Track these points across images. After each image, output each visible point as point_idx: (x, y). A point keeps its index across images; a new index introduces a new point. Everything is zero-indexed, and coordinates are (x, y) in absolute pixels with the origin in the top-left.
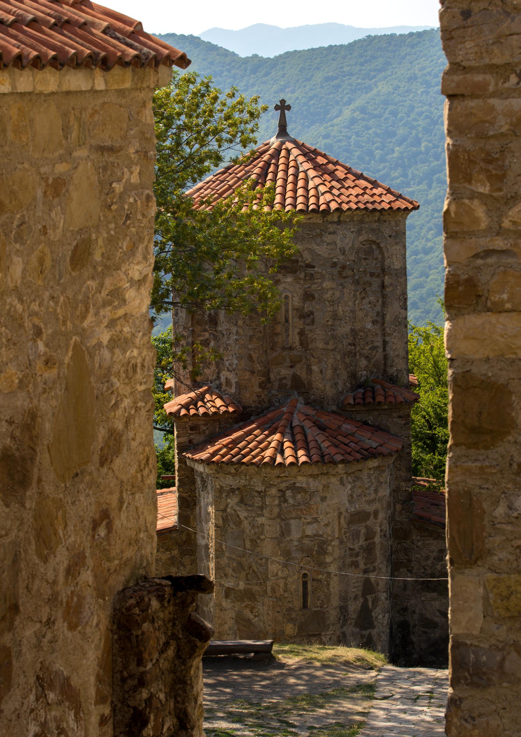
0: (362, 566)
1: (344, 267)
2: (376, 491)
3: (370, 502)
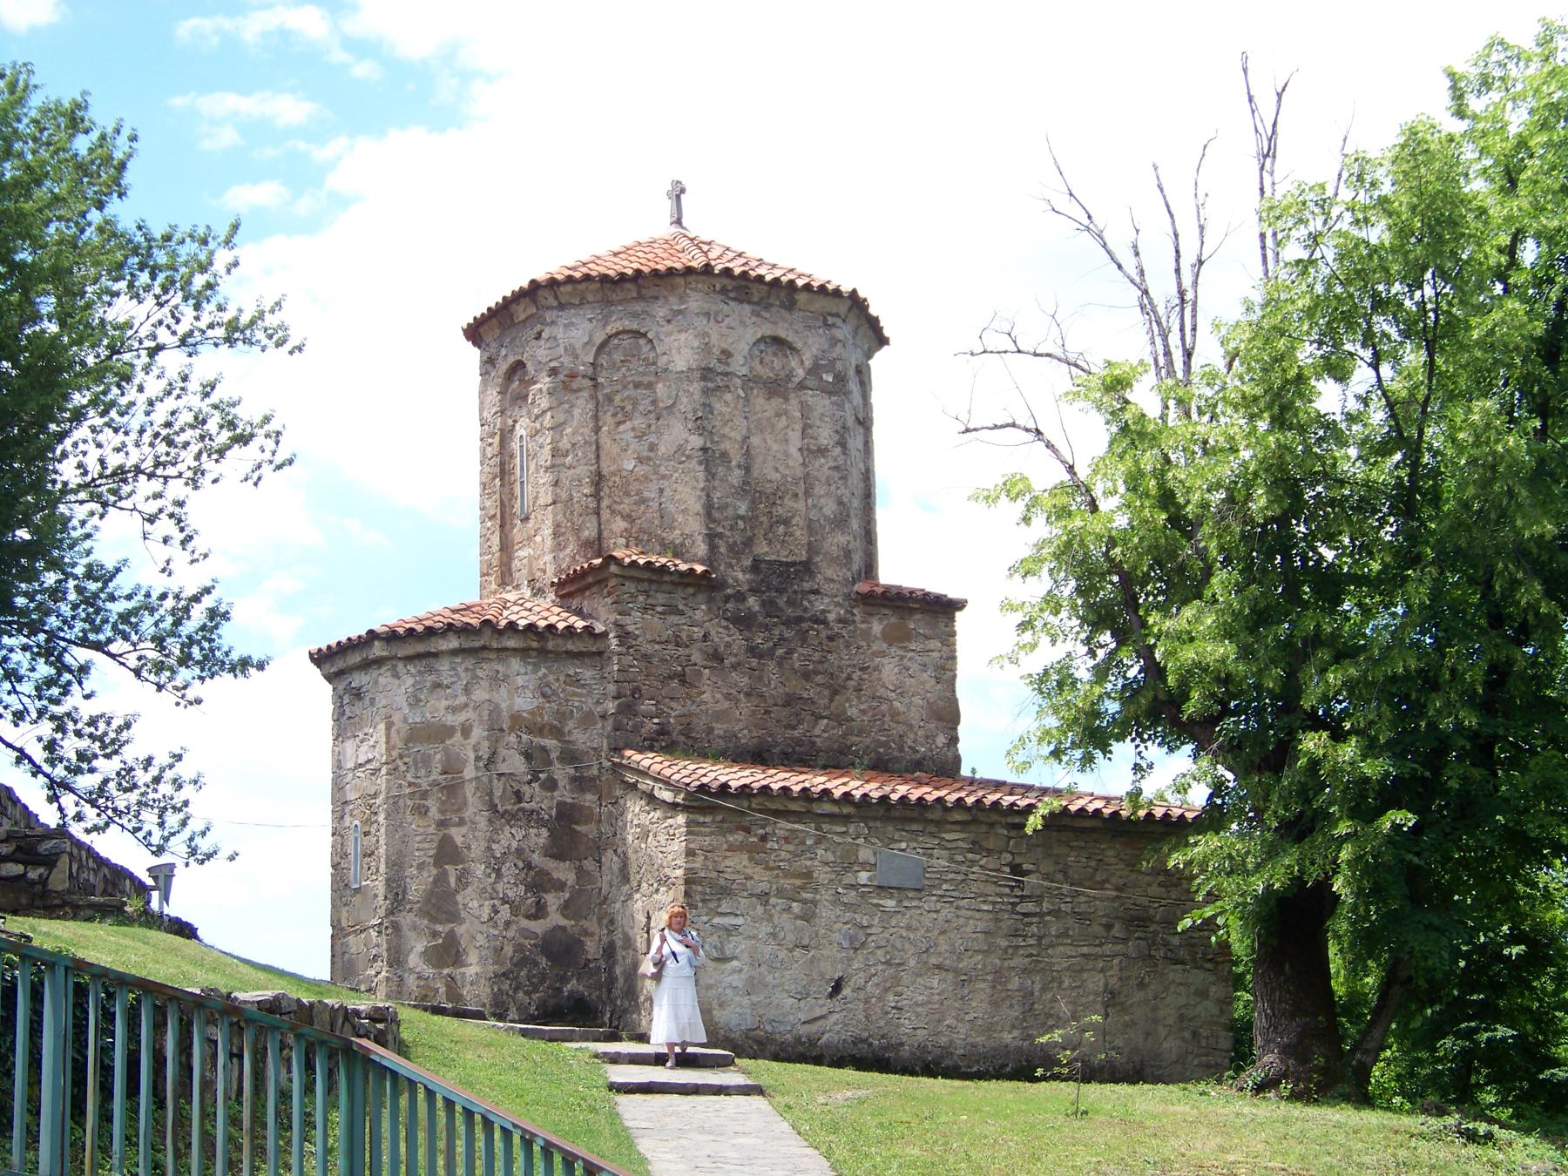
0: (434, 812)
1: (572, 376)
2: (467, 690)
3: (454, 710)
